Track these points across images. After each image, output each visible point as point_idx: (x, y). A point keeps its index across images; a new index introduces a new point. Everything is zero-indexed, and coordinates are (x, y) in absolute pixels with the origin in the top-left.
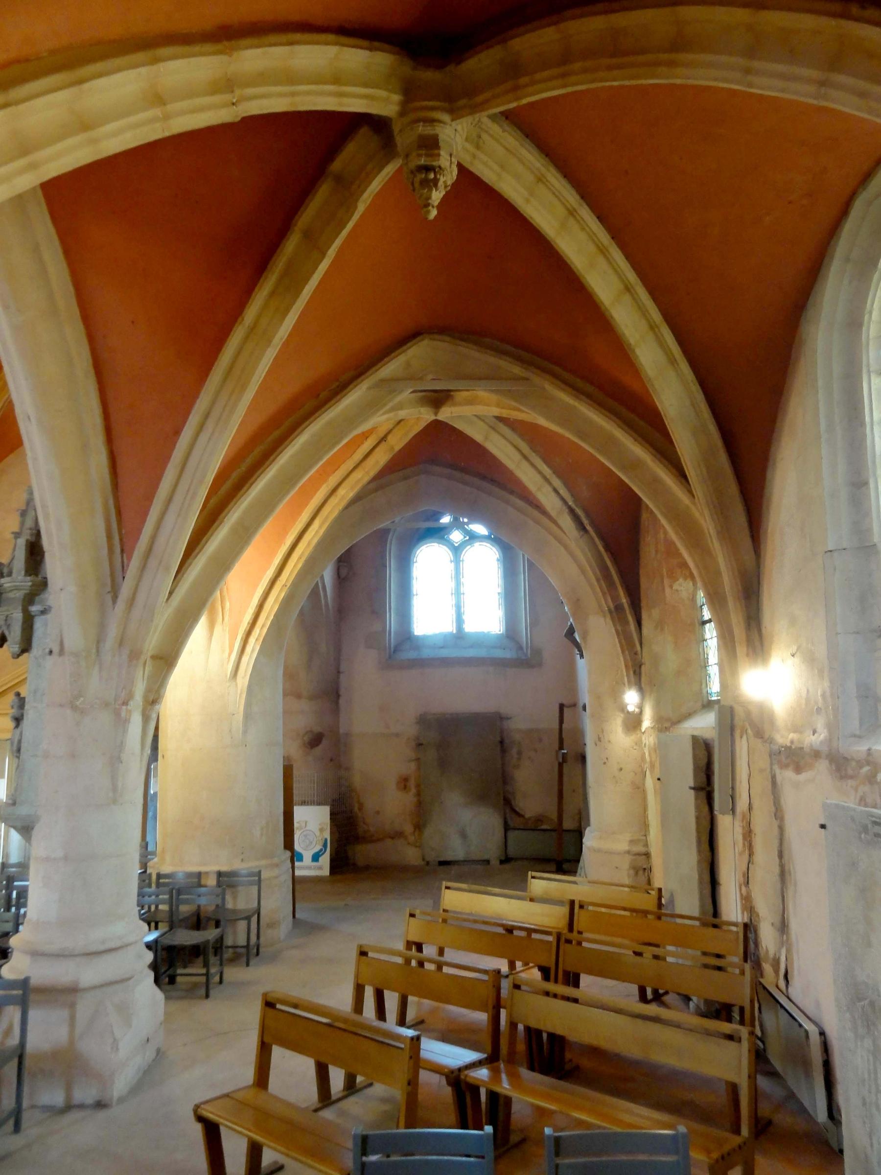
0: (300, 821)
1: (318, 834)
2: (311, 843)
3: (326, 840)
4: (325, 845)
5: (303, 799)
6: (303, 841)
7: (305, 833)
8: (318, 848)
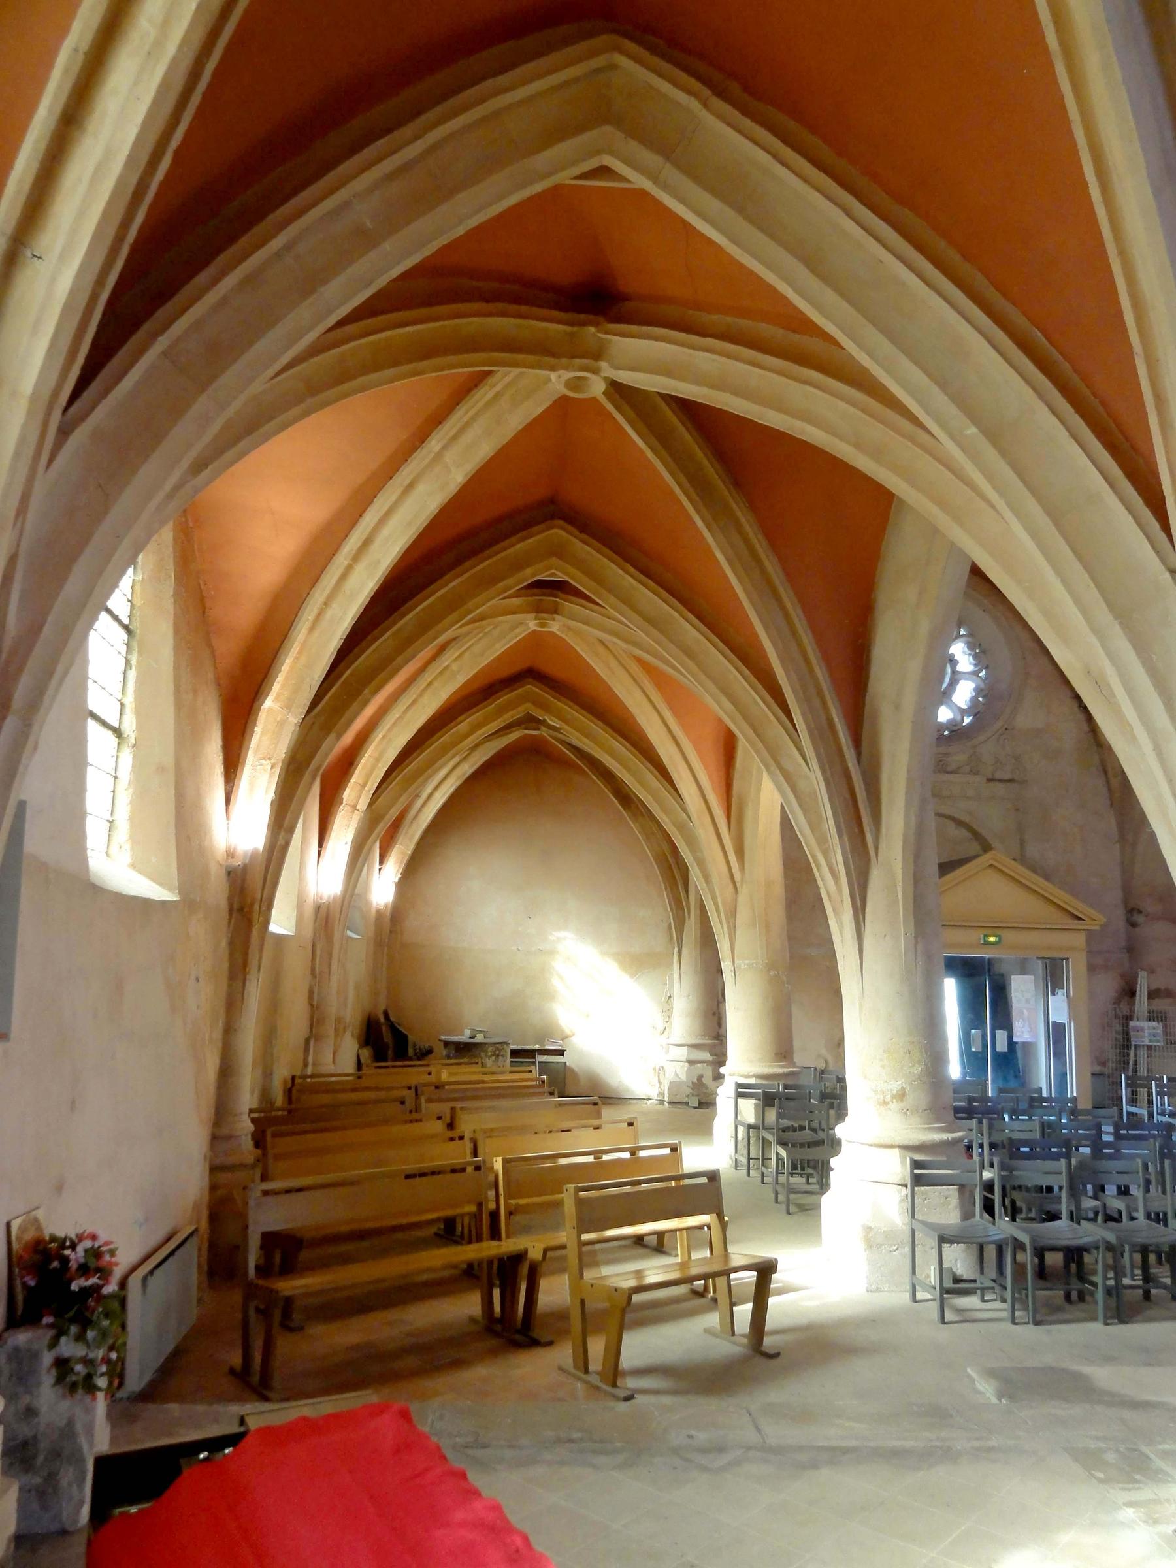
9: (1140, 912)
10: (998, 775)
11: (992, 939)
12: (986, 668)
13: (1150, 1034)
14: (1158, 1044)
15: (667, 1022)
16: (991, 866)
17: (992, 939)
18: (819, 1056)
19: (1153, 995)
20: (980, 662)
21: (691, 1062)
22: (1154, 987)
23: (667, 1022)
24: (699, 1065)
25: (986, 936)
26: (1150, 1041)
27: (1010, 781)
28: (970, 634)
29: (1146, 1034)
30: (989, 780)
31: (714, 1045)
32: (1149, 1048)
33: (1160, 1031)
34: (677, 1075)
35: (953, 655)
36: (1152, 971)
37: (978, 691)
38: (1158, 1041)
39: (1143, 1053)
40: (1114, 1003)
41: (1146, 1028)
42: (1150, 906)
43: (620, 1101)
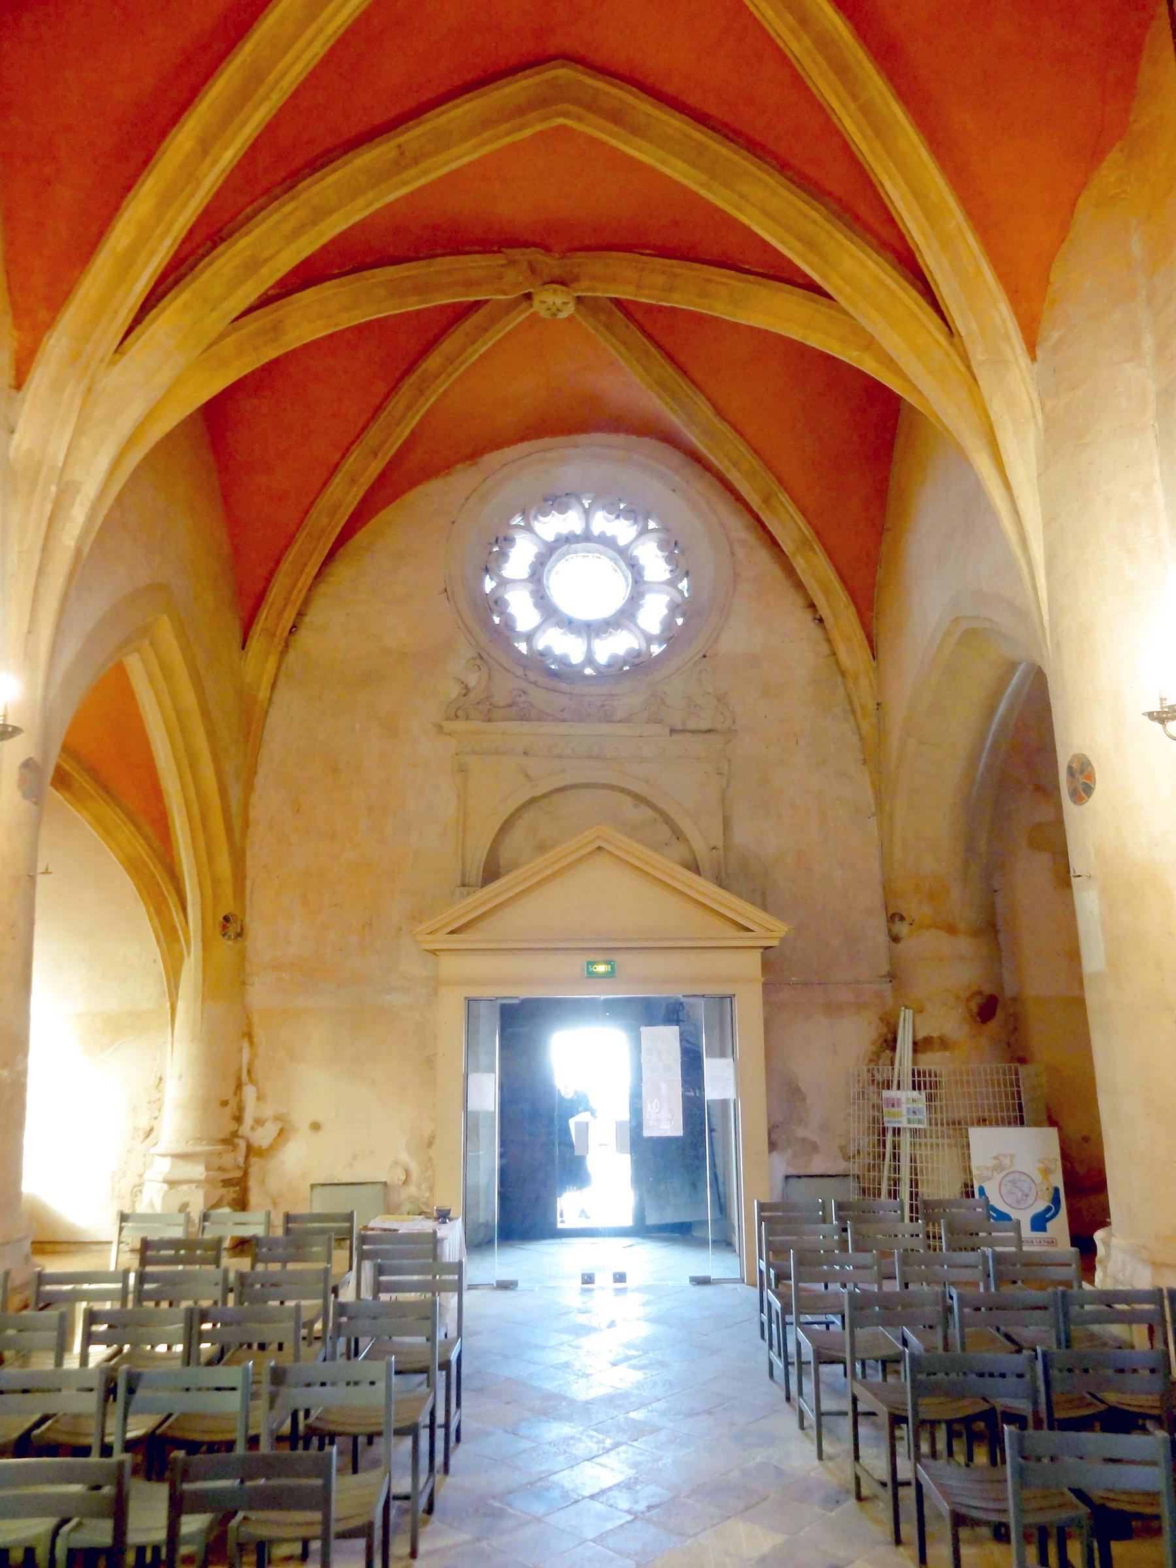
0: (998, 1156)
1: (1038, 1178)
2: (1027, 1196)
3: (1057, 1190)
4: (1056, 1200)
5: (981, 1114)
6: (1010, 1193)
7: (1011, 1177)
8: (1041, 1205)
9: (902, 918)
10: (693, 724)
11: (601, 968)
12: (687, 574)
13: (908, 1109)
14: (921, 1126)
15: (156, 1118)
16: (600, 848)
17: (601, 968)
18: (396, 1163)
19: (918, 1047)
20: (677, 567)
21: (172, 1183)
22: (921, 1035)
23: (156, 1118)
24: (185, 1187)
25: (592, 963)
26: (909, 1121)
27: (709, 731)
28: (665, 529)
29: (904, 1112)
30: (673, 731)
31: (209, 1154)
32: (915, 1132)
33: (922, 1105)
34: (152, 1205)
35: (636, 558)
36: (919, 1010)
37: (675, 608)
38: (920, 1122)
39: (905, 1140)
40: (871, 1061)
41: (904, 1100)
42: (914, 907)
43: (74, 1247)
